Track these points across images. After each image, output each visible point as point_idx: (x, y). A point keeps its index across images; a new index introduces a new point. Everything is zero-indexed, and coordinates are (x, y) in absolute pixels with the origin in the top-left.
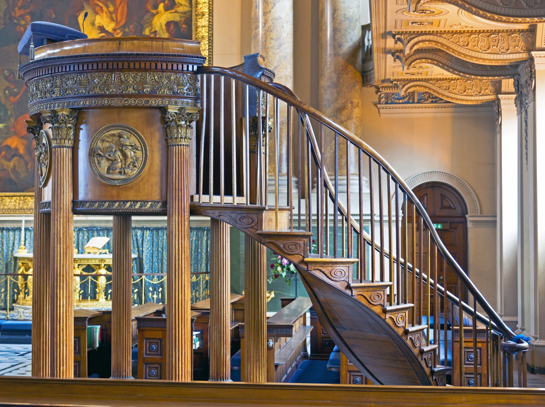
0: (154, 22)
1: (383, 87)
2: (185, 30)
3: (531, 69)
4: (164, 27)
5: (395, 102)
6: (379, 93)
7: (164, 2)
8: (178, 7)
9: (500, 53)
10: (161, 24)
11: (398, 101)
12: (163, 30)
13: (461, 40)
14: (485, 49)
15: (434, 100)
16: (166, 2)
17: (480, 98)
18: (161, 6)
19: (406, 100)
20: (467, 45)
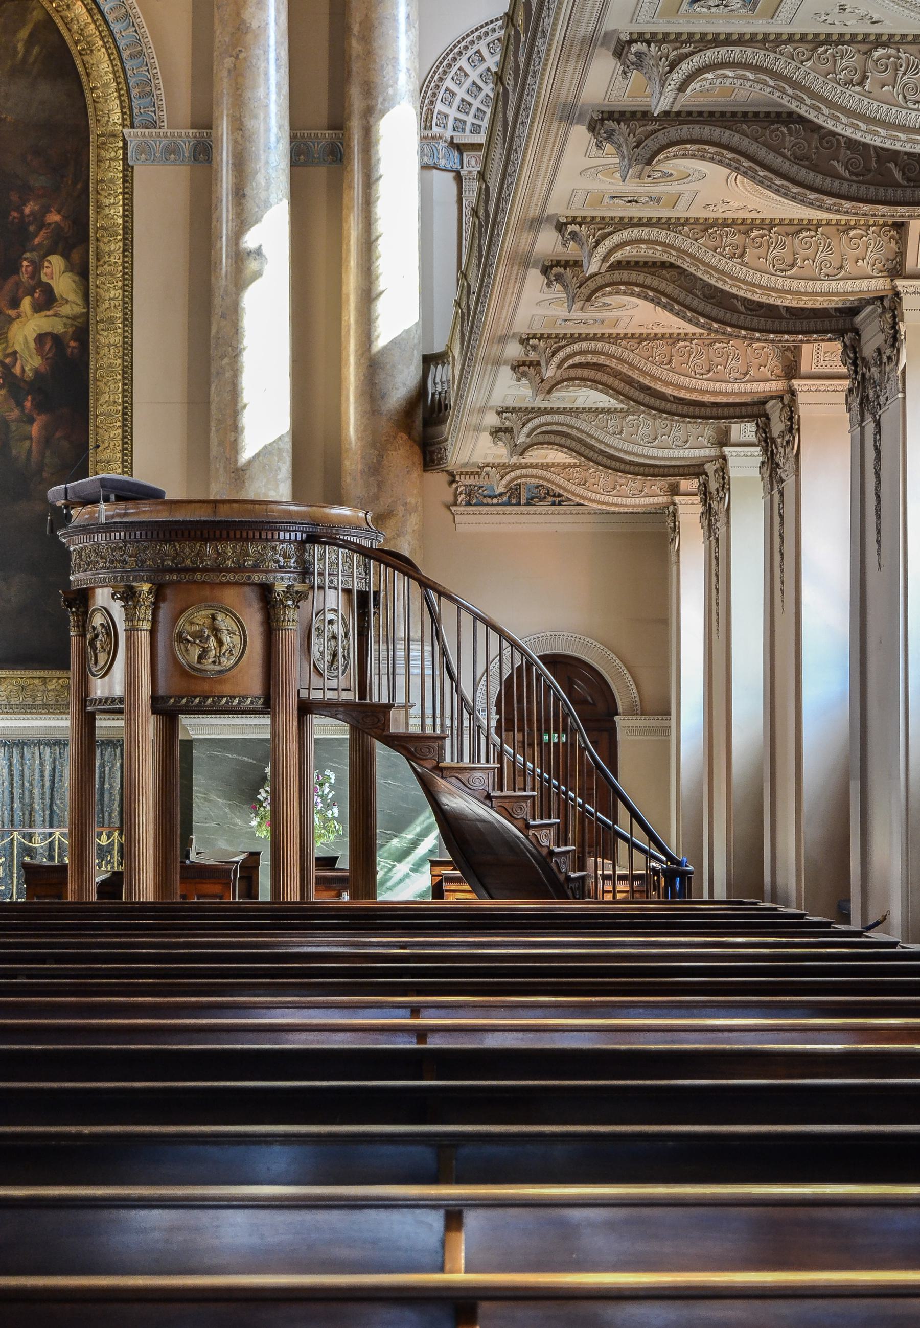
0: (11, 334)
1: (461, 473)
2: (76, 351)
3: (724, 473)
4: (32, 345)
5: (485, 502)
6: (455, 485)
7: (32, 296)
8: (61, 305)
9: (674, 447)
10: (25, 338)
11: (489, 501)
12: (29, 350)
13: (610, 424)
14: (650, 440)
15: (557, 500)
16: (36, 295)
17: (643, 501)
18: (26, 303)
19: (505, 499)
20: (620, 433)
